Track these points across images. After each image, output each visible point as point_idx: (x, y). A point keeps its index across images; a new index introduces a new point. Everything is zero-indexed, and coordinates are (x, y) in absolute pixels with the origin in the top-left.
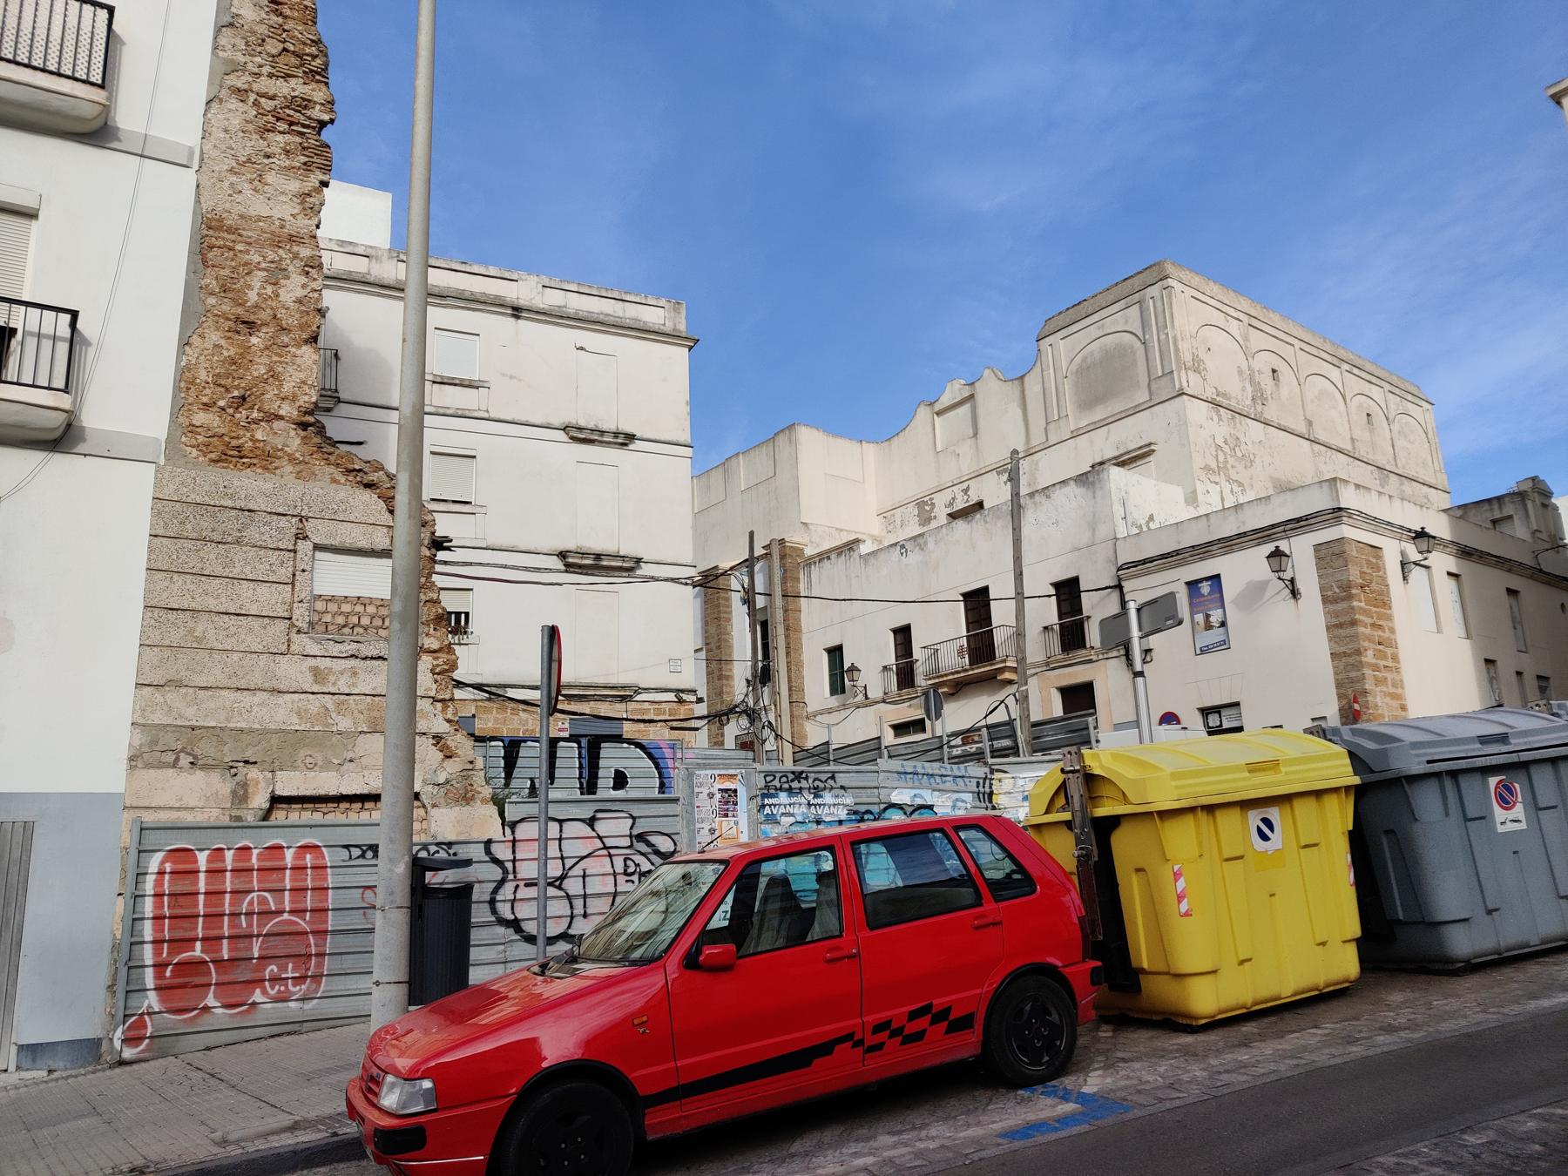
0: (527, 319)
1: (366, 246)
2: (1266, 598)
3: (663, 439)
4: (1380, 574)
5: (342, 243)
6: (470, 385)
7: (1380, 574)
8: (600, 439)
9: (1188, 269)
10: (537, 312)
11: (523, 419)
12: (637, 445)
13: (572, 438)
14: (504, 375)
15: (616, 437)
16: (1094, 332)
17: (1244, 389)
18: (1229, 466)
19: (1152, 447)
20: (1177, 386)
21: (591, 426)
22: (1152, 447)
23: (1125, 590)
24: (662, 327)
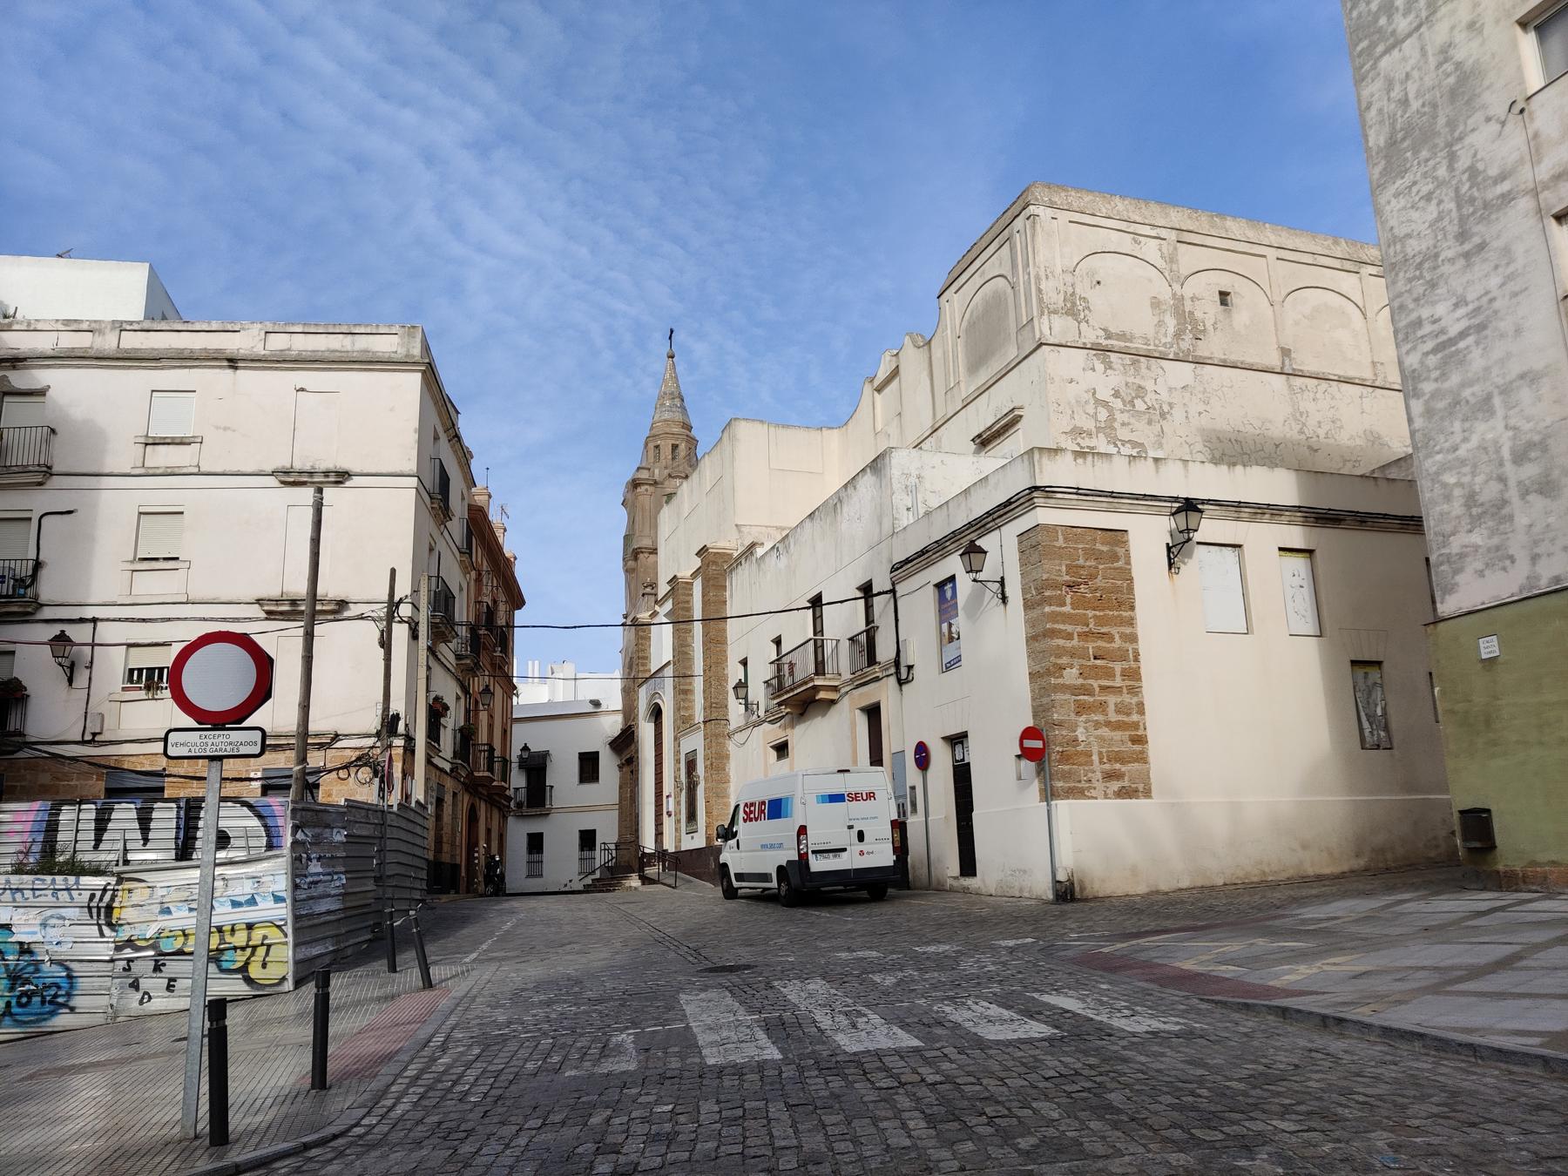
0: (245, 368)
1: (90, 321)
2: (985, 604)
3: (384, 471)
4: (1120, 564)
5: (67, 322)
6: (182, 442)
7: (1120, 564)
8: (310, 480)
9: (1073, 188)
10: (252, 360)
11: (234, 469)
12: (356, 481)
13: (282, 482)
14: (218, 428)
15: (327, 476)
16: (977, 280)
17: (1160, 323)
18: (1116, 425)
19: (1016, 413)
20: (1038, 336)
21: (307, 468)
22: (1016, 413)
23: (898, 595)
24: (393, 355)
